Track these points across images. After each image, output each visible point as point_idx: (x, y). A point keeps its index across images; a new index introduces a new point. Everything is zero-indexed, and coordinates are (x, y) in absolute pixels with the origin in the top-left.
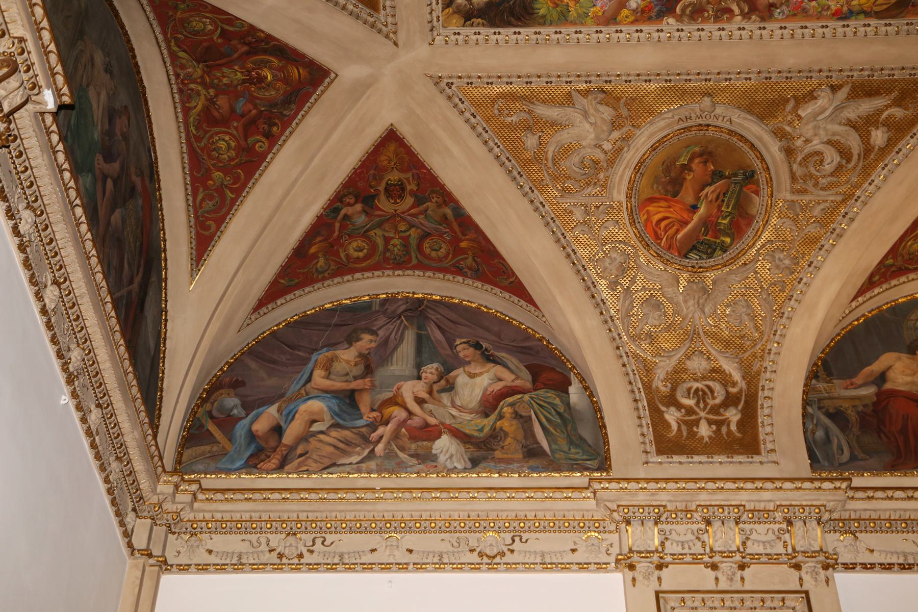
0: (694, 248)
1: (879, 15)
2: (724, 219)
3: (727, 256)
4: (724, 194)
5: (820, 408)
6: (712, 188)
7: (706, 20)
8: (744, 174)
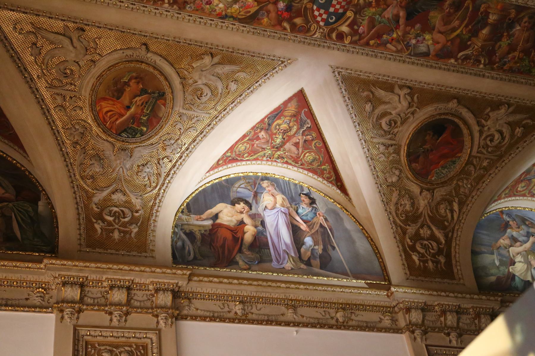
0: (125, 131)
1: (241, 21)
2: (145, 116)
3: (143, 138)
4: (146, 103)
5: (181, 229)
6: (140, 98)
8: (159, 93)
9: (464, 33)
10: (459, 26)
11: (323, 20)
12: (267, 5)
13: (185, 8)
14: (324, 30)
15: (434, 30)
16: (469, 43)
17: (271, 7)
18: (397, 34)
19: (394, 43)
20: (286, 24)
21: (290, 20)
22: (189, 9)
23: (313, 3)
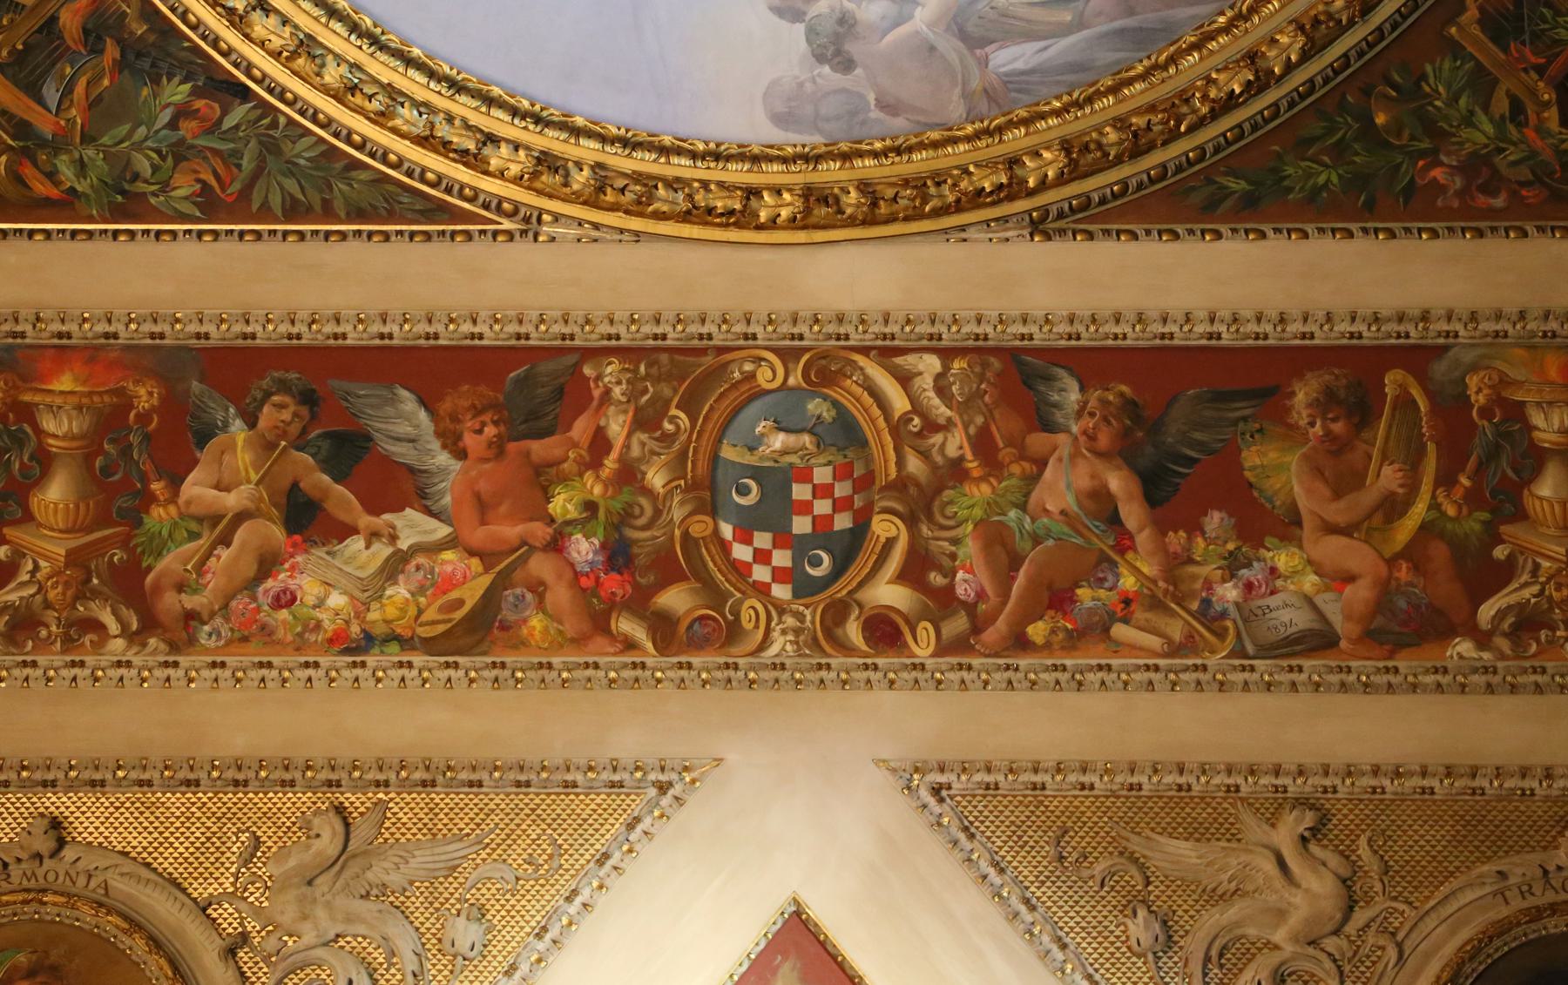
1: (430, 646)
7: (43, 645)
9: (1451, 511)
10: (1413, 489)
11: (780, 575)
12: (524, 560)
13: (192, 641)
14: (800, 617)
15: (1298, 523)
16: (1500, 552)
17: (541, 566)
18: (1136, 571)
19: (1140, 615)
20: (626, 625)
21: (639, 604)
22: (212, 643)
23: (714, 513)
